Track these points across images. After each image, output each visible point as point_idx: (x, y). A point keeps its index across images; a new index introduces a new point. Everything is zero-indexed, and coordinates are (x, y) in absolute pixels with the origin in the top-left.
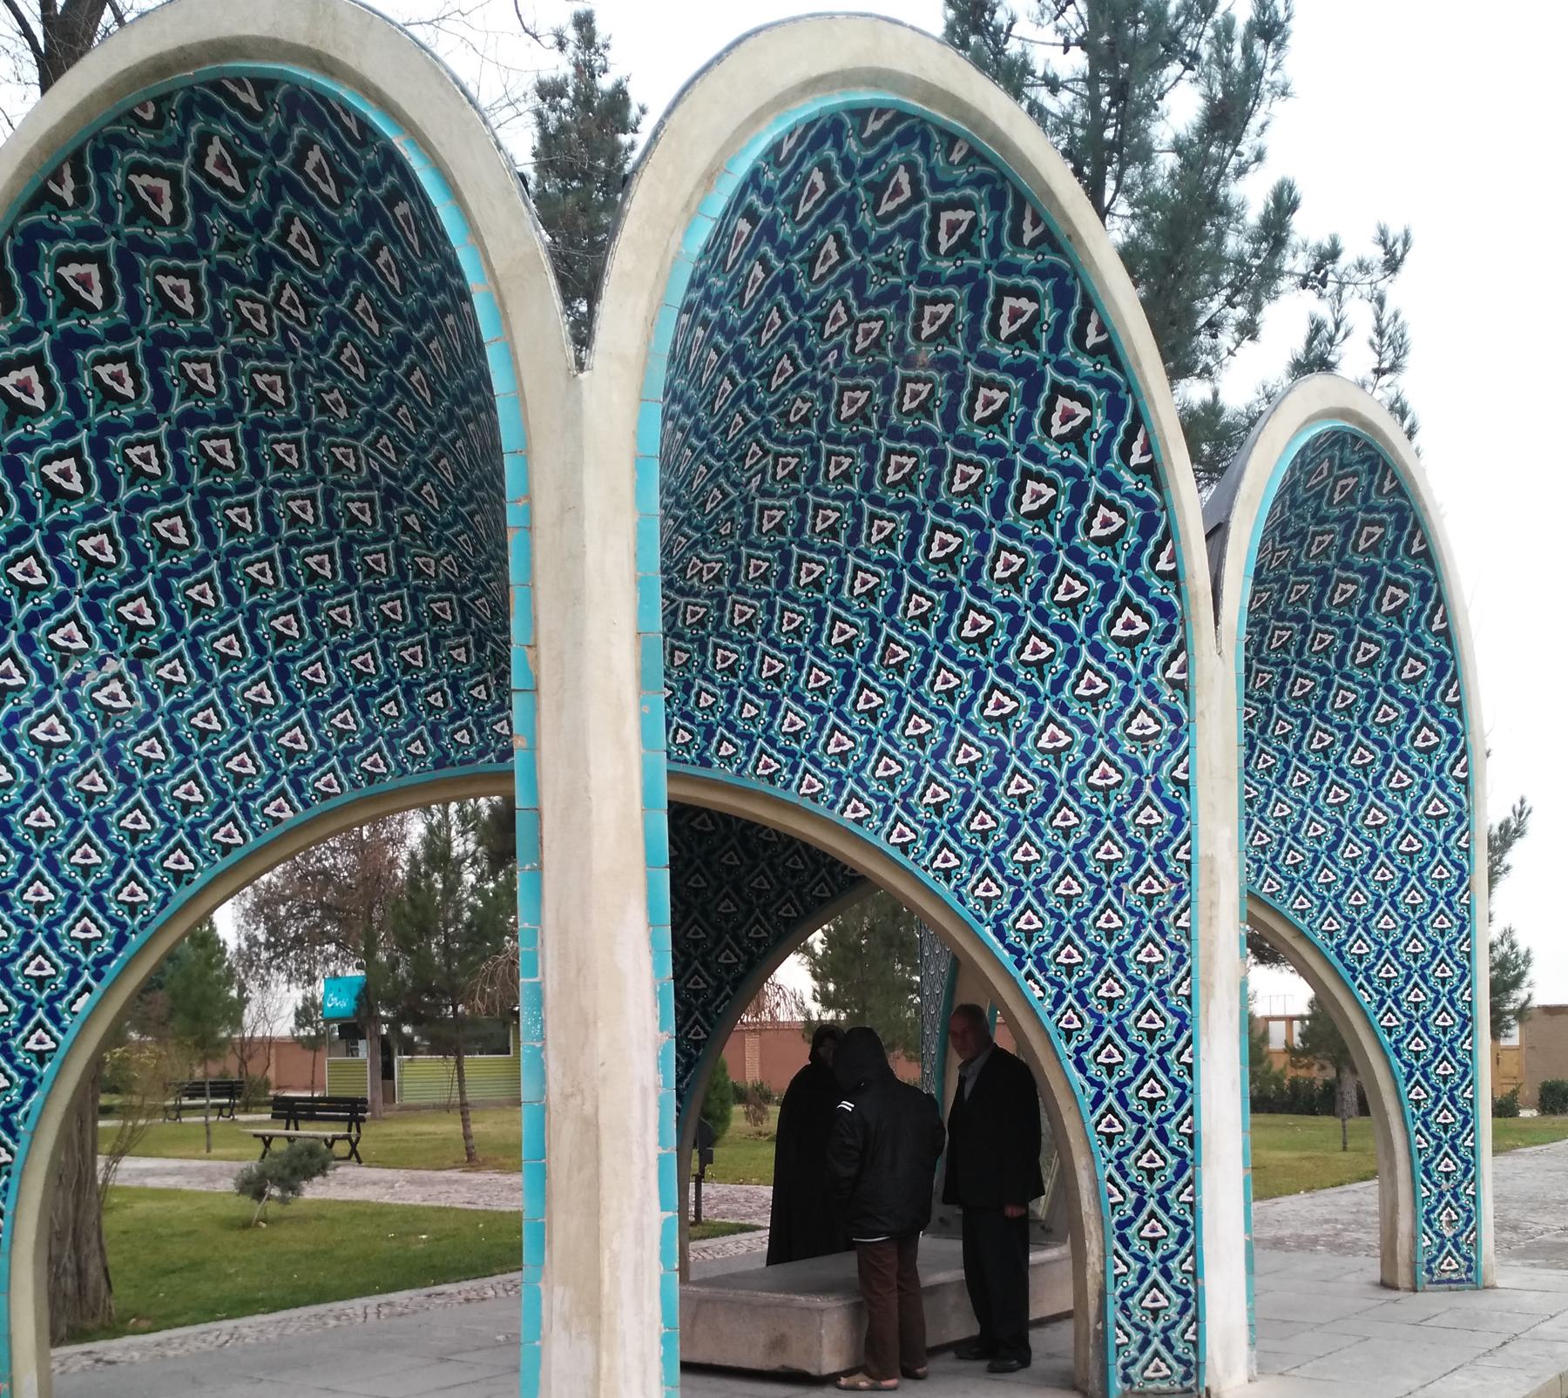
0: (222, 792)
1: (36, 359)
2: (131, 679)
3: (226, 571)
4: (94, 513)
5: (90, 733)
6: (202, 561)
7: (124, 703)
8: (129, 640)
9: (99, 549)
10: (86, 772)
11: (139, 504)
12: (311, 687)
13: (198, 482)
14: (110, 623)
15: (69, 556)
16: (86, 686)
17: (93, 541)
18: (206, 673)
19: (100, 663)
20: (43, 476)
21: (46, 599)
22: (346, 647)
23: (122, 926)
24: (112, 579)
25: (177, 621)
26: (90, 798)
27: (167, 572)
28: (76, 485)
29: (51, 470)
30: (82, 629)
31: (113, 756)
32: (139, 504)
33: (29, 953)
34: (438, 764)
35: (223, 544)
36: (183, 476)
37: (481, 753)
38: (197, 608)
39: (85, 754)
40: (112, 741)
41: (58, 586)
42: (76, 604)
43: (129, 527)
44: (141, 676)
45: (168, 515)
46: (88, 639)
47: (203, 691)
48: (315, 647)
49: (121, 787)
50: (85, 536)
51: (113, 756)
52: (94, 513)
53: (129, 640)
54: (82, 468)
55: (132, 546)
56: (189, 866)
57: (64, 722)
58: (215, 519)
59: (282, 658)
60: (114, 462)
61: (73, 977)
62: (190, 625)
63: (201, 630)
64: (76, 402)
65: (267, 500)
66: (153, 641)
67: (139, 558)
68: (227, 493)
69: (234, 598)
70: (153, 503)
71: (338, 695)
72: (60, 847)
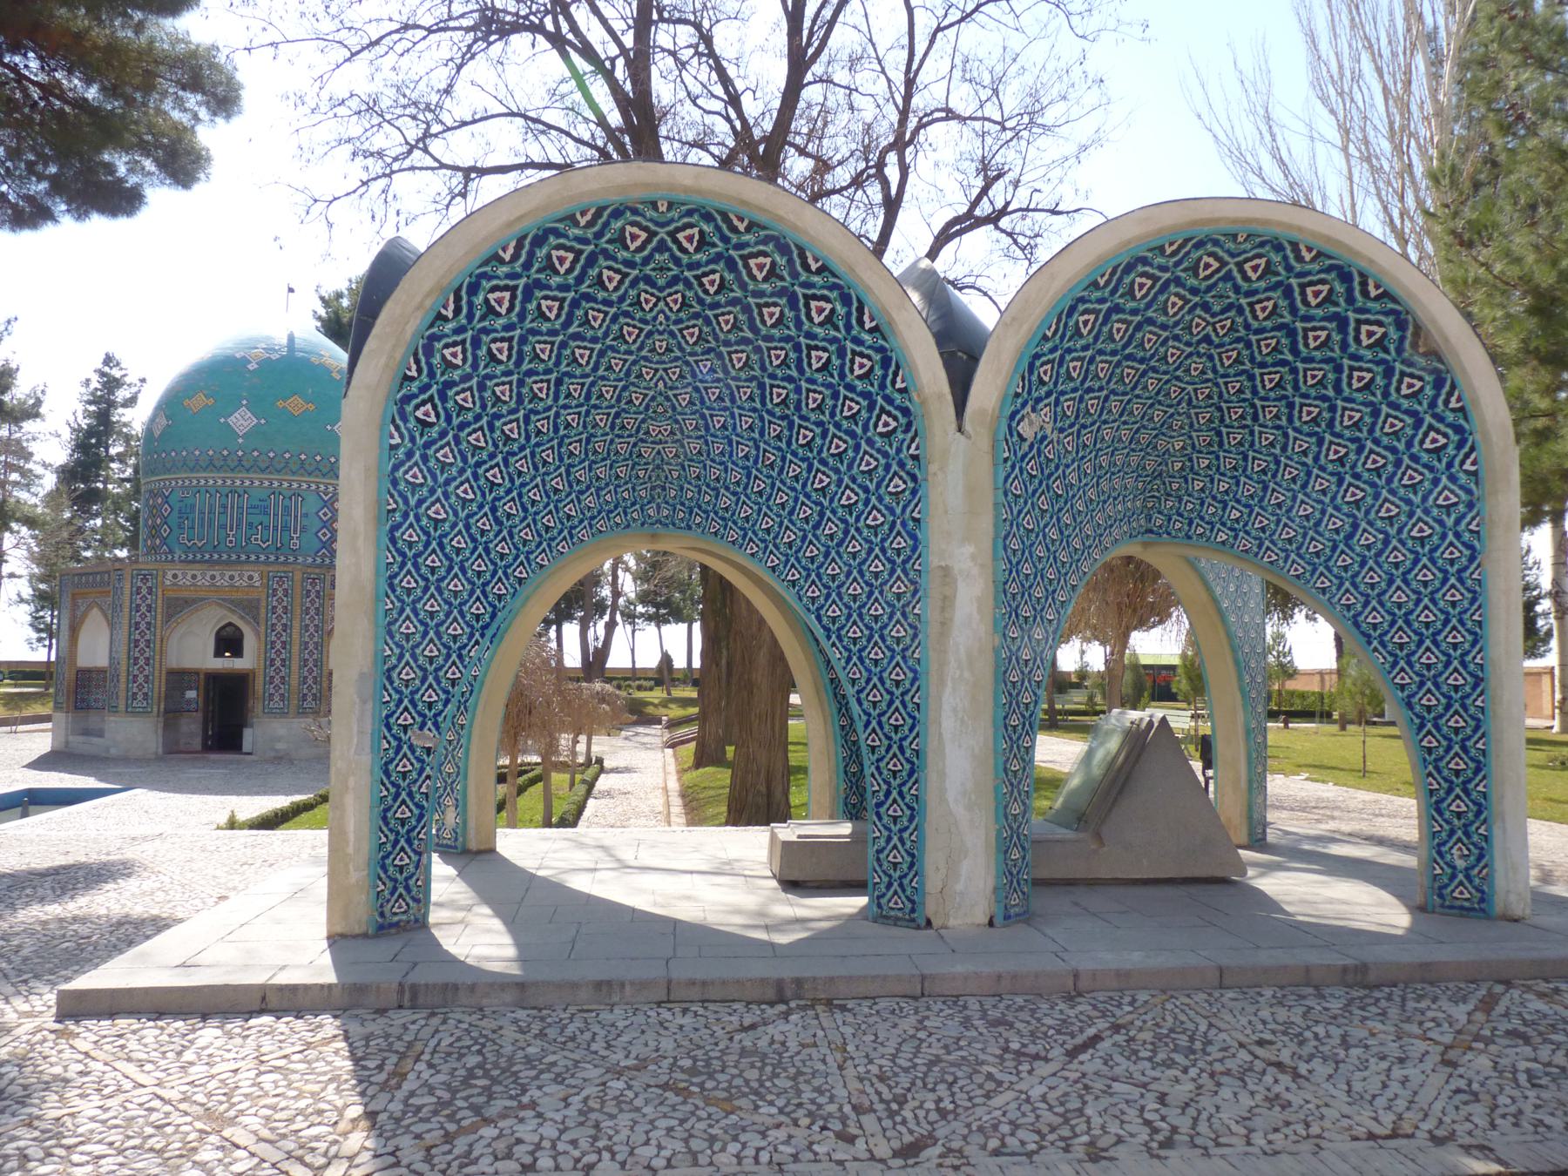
1: (513, 289)
3: (557, 415)
5: (483, 495)
9: (503, 393)
11: (530, 373)
12: (579, 481)
13: (563, 368)
15: (487, 394)
18: (536, 468)
23: (494, 607)
25: (528, 438)
26: (483, 532)
27: (531, 411)
31: (494, 510)
32: (530, 373)
35: (561, 402)
36: (558, 363)
38: (539, 432)
39: (481, 507)
51: (494, 510)
54: (510, 349)
60: (527, 348)
61: (471, 636)
63: (538, 445)
64: (522, 316)
67: (520, 401)
69: (556, 430)
70: (537, 374)
71: (588, 488)
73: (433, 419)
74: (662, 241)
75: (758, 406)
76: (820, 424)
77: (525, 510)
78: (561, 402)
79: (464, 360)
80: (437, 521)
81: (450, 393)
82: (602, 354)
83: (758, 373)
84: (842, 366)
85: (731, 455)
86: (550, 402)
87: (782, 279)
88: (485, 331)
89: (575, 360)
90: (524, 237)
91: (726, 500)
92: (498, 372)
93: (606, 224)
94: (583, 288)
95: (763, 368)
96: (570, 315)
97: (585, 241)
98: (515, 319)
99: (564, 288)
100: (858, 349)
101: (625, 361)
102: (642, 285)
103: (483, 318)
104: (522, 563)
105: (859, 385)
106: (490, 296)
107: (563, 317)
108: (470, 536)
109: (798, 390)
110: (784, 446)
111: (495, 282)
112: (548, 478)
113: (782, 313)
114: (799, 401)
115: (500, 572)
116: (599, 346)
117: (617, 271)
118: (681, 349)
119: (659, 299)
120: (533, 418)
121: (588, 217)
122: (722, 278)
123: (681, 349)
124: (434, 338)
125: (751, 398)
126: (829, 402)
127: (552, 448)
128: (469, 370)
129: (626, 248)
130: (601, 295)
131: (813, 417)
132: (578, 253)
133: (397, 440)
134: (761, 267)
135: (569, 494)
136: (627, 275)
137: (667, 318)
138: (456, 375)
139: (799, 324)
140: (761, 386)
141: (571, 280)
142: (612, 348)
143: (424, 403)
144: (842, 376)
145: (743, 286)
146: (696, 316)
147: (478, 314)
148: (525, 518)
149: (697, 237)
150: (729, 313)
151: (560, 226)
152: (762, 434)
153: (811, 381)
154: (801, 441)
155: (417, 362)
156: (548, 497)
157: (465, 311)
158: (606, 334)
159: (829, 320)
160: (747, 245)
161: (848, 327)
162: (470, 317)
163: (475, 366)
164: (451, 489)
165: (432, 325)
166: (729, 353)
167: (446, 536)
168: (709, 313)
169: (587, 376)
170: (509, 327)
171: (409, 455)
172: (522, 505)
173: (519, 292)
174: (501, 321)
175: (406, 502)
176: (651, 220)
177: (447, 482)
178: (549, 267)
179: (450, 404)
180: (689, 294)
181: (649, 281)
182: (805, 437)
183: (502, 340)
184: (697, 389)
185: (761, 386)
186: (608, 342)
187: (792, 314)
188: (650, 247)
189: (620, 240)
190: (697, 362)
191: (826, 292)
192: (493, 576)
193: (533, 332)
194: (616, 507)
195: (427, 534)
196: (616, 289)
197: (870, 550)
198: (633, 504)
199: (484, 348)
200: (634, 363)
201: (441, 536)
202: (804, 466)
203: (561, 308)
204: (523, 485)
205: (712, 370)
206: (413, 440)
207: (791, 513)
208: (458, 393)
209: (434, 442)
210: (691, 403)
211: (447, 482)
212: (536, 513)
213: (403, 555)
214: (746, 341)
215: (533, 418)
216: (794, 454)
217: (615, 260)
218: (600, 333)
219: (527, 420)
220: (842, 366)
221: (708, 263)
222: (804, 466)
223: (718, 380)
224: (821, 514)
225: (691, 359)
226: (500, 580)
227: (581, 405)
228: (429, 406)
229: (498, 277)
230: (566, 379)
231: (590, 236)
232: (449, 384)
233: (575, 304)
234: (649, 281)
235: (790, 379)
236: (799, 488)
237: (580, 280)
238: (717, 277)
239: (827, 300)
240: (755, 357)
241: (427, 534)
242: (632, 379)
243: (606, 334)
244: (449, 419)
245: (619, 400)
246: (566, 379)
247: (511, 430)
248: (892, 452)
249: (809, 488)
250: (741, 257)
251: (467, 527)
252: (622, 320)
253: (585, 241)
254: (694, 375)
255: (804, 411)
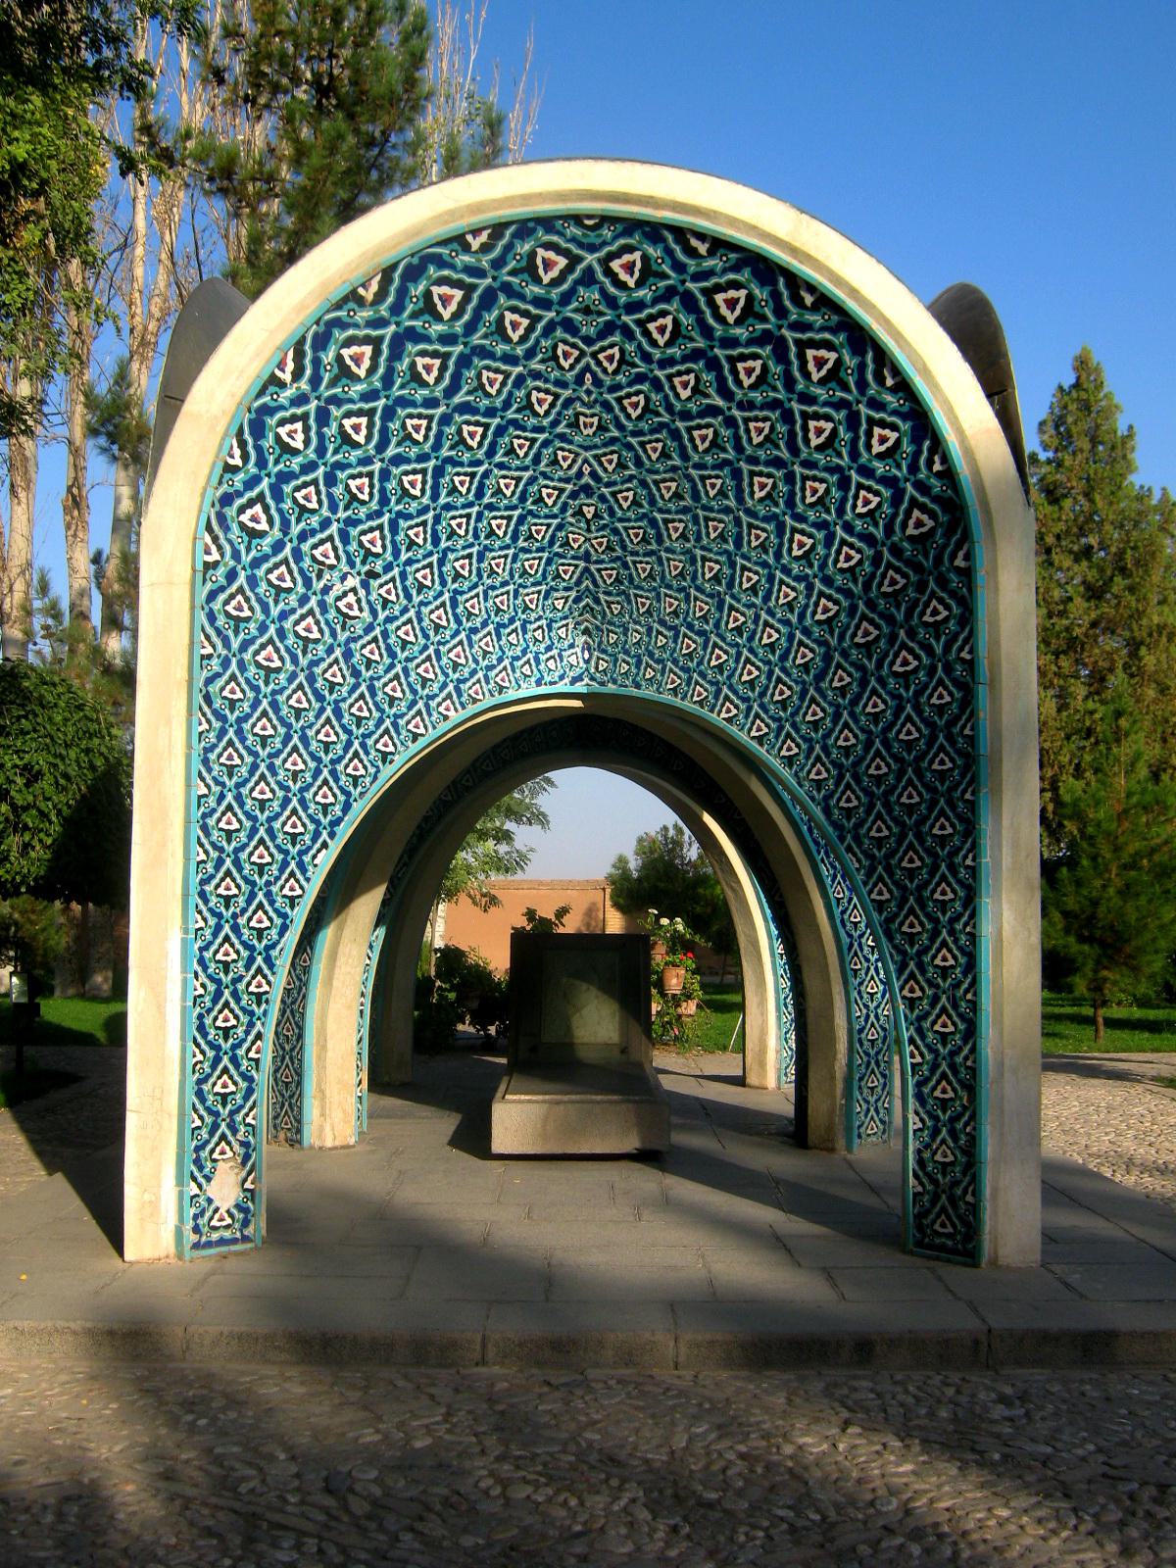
0: (414, 692)
2: (362, 593)
3: (437, 519)
4: (366, 461)
5: (334, 634)
6: (425, 510)
7: (355, 613)
8: (363, 563)
9: (360, 489)
10: (330, 666)
11: (398, 460)
13: (445, 452)
14: (353, 546)
15: (338, 491)
16: (333, 594)
17: (358, 481)
18: (408, 597)
19: (343, 578)
20: (341, 426)
21: (315, 522)
22: (493, 588)
23: (348, 794)
24: (363, 512)
25: (396, 554)
26: (332, 686)
27: (400, 514)
28: (360, 438)
29: (347, 423)
30: (335, 549)
31: (348, 655)
32: (398, 460)
33: (287, 813)
34: (539, 683)
35: (443, 500)
36: (437, 447)
37: (562, 678)
38: (412, 544)
39: (330, 651)
40: (349, 641)
41: (325, 512)
42: (334, 529)
43: (385, 475)
44: (368, 593)
45: (414, 472)
46: (337, 557)
47: (405, 610)
48: (475, 586)
49: (353, 681)
50: (353, 477)
51: (348, 655)
52: (366, 461)
53: (363, 563)
54: (370, 426)
55: (383, 491)
56: (391, 749)
57: (317, 623)
58: (444, 481)
59: (456, 592)
62: (404, 557)
63: (409, 562)
65: (486, 474)
66: (379, 569)
67: (384, 501)
68: (461, 464)
69: (436, 541)
70: (408, 461)
71: (485, 624)
72: (310, 726)
73: (263, 526)
74: (589, 270)
75: (732, 503)
76: (822, 525)
77: (392, 655)
78: (443, 500)
79: (307, 442)
80: (269, 671)
81: (287, 489)
82: (500, 431)
83: (731, 455)
84: (854, 441)
85: (694, 578)
86: (426, 500)
87: (764, 319)
88: (336, 401)
89: (463, 441)
90: (393, 267)
91: (688, 645)
92: (353, 459)
93: (509, 247)
94: (476, 339)
95: (739, 449)
96: (457, 378)
97: (479, 273)
98: (378, 385)
99: (448, 339)
100: (877, 416)
101: (533, 441)
102: (559, 333)
103: (333, 383)
104: (387, 731)
105: (880, 468)
106: (345, 352)
107: (446, 382)
108: (316, 692)
109: (790, 478)
110: (771, 561)
111: (351, 332)
112: (425, 610)
113: (764, 367)
114: (792, 494)
115: (356, 745)
116: (496, 421)
117: (525, 314)
118: (620, 427)
119: (583, 354)
120: (403, 524)
121: (484, 237)
122: (676, 322)
123: (620, 427)
124: (267, 410)
125: (722, 493)
126: (835, 493)
127: (430, 565)
128: (313, 456)
129: (538, 280)
130: (501, 348)
131: (811, 515)
132: (469, 289)
133: (215, 556)
134: (731, 304)
135: (457, 633)
136: (539, 318)
137: (597, 382)
138: (296, 464)
139: (790, 383)
140: (737, 474)
141: (458, 327)
142: (514, 423)
143: (251, 503)
144: (854, 455)
145: (707, 332)
146: (640, 378)
147: (327, 377)
148: (392, 666)
149: (639, 265)
150: (688, 372)
151: (444, 251)
152: (738, 544)
153: (808, 464)
154: (796, 552)
155: (242, 444)
156: (426, 636)
157: (308, 372)
158: (507, 405)
159: (834, 376)
160: (710, 273)
161: (862, 385)
162: (315, 381)
163: (321, 451)
164: (288, 624)
165: (261, 393)
166: (689, 430)
167: (281, 691)
168: (660, 374)
169: (479, 463)
170: (370, 396)
171: (232, 576)
172: (389, 648)
173: (385, 347)
174: (360, 387)
175: (227, 644)
176: (573, 240)
177: (284, 615)
178: (428, 308)
179: (287, 505)
180: (630, 347)
181: (569, 326)
182: (801, 545)
183: (360, 413)
184: (643, 484)
185: (737, 474)
186: (510, 414)
187: (779, 369)
188: (571, 278)
189: (530, 269)
190: (643, 444)
191: (827, 336)
192: (346, 750)
193: (403, 402)
194: (524, 652)
195: (256, 689)
196: (523, 339)
197: (899, 709)
198: (549, 649)
199: (334, 425)
200: (546, 444)
201: (274, 693)
202: (802, 587)
203: (443, 368)
204: (389, 620)
205: (665, 455)
206: (236, 555)
207: (784, 658)
208: (297, 489)
209: (266, 558)
210: (636, 503)
211: (284, 615)
212: (408, 660)
213: (223, 719)
214: (713, 411)
215: (403, 524)
216: (786, 570)
217: (522, 297)
218: (498, 403)
219: (394, 527)
220: (854, 441)
221: (656, 301)
222: (802, 587)
223: (674, 469)
224: (827, 658)
225: (633, 441)
226: (356, 755)
227: (471, 505)
228: (258, 508)
229: (356, 326)
230: (449, 468)
231: (485, 264)
232: (285, 477)
233: (464, 361)
234: (569, 326)
235: (778, 463)
236: (794, 619)
237: (471, 328)
238: (668, 321)
239: (829, 346)
240: (725, 433)
241: (256, 689)
242: (542, 467)
243: (507, 405)
244: (285, 527)
245: (523, 498)
246: (449, 468)
247: (372, 542)
248: (928, 564)
249: (808, 621)
250: (705, 292)
251: (311, 679)
252: (531, 383)
253: (479, 273)
254: (639, 463)
255: (800, 508)
